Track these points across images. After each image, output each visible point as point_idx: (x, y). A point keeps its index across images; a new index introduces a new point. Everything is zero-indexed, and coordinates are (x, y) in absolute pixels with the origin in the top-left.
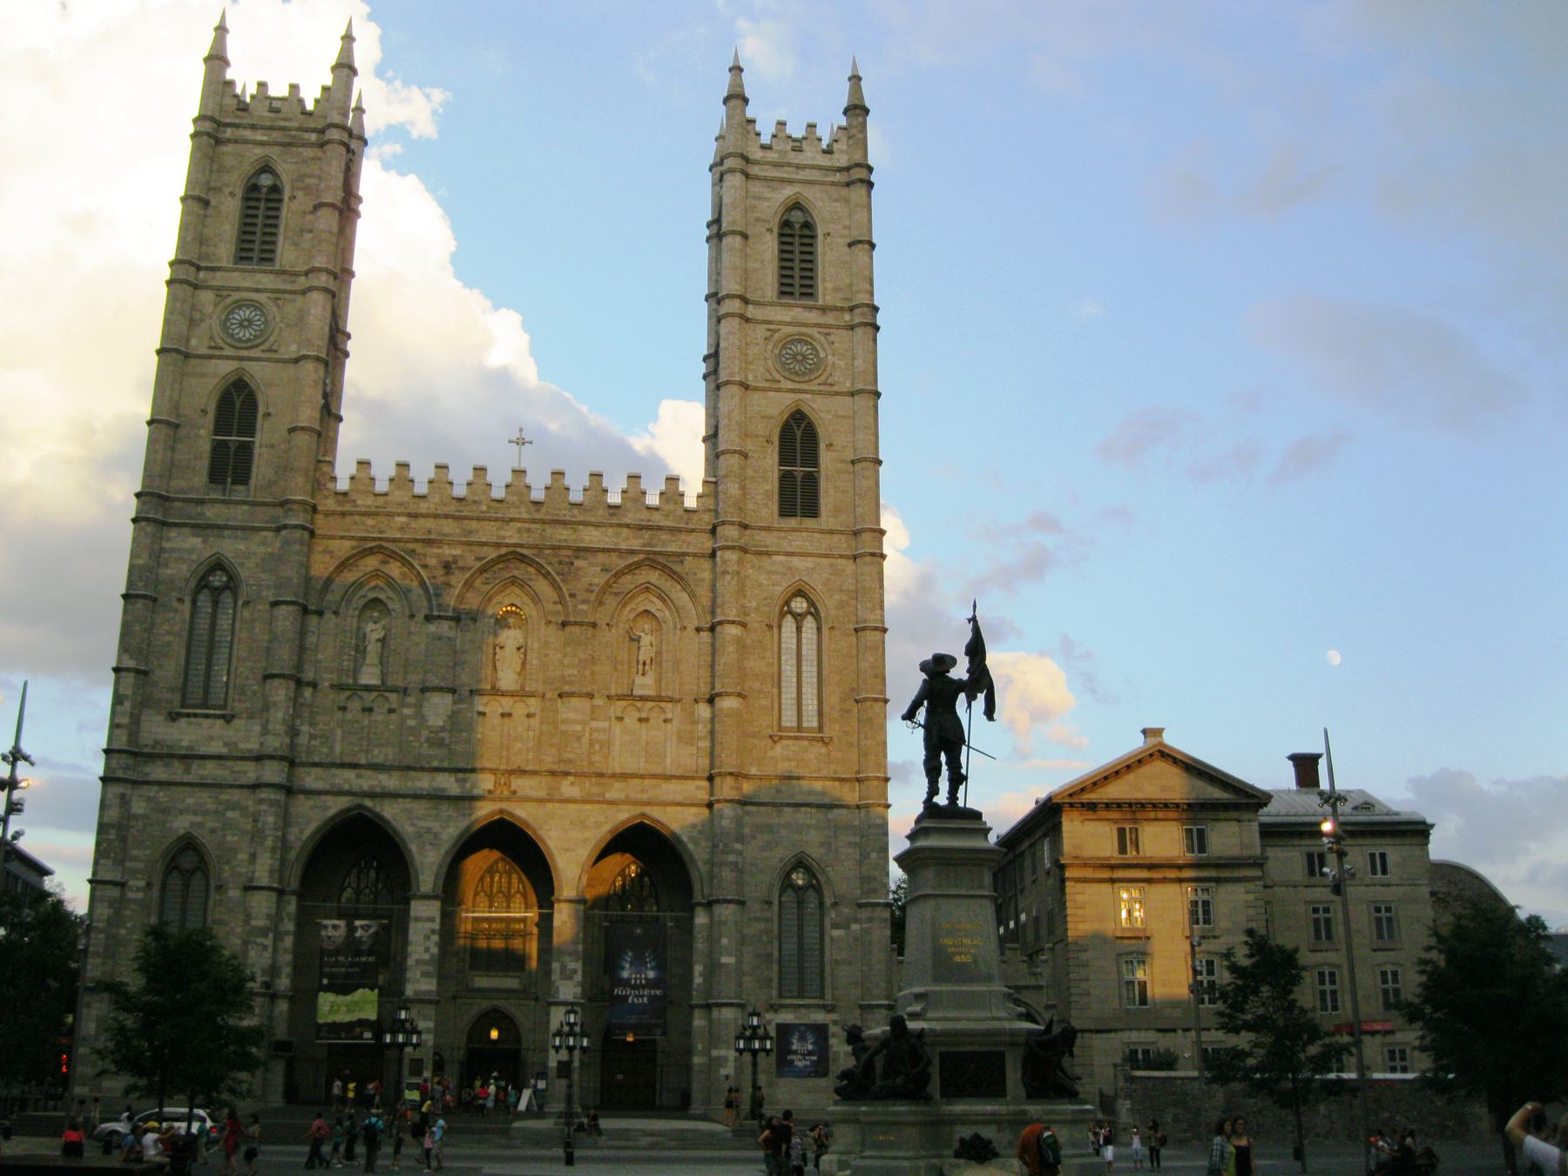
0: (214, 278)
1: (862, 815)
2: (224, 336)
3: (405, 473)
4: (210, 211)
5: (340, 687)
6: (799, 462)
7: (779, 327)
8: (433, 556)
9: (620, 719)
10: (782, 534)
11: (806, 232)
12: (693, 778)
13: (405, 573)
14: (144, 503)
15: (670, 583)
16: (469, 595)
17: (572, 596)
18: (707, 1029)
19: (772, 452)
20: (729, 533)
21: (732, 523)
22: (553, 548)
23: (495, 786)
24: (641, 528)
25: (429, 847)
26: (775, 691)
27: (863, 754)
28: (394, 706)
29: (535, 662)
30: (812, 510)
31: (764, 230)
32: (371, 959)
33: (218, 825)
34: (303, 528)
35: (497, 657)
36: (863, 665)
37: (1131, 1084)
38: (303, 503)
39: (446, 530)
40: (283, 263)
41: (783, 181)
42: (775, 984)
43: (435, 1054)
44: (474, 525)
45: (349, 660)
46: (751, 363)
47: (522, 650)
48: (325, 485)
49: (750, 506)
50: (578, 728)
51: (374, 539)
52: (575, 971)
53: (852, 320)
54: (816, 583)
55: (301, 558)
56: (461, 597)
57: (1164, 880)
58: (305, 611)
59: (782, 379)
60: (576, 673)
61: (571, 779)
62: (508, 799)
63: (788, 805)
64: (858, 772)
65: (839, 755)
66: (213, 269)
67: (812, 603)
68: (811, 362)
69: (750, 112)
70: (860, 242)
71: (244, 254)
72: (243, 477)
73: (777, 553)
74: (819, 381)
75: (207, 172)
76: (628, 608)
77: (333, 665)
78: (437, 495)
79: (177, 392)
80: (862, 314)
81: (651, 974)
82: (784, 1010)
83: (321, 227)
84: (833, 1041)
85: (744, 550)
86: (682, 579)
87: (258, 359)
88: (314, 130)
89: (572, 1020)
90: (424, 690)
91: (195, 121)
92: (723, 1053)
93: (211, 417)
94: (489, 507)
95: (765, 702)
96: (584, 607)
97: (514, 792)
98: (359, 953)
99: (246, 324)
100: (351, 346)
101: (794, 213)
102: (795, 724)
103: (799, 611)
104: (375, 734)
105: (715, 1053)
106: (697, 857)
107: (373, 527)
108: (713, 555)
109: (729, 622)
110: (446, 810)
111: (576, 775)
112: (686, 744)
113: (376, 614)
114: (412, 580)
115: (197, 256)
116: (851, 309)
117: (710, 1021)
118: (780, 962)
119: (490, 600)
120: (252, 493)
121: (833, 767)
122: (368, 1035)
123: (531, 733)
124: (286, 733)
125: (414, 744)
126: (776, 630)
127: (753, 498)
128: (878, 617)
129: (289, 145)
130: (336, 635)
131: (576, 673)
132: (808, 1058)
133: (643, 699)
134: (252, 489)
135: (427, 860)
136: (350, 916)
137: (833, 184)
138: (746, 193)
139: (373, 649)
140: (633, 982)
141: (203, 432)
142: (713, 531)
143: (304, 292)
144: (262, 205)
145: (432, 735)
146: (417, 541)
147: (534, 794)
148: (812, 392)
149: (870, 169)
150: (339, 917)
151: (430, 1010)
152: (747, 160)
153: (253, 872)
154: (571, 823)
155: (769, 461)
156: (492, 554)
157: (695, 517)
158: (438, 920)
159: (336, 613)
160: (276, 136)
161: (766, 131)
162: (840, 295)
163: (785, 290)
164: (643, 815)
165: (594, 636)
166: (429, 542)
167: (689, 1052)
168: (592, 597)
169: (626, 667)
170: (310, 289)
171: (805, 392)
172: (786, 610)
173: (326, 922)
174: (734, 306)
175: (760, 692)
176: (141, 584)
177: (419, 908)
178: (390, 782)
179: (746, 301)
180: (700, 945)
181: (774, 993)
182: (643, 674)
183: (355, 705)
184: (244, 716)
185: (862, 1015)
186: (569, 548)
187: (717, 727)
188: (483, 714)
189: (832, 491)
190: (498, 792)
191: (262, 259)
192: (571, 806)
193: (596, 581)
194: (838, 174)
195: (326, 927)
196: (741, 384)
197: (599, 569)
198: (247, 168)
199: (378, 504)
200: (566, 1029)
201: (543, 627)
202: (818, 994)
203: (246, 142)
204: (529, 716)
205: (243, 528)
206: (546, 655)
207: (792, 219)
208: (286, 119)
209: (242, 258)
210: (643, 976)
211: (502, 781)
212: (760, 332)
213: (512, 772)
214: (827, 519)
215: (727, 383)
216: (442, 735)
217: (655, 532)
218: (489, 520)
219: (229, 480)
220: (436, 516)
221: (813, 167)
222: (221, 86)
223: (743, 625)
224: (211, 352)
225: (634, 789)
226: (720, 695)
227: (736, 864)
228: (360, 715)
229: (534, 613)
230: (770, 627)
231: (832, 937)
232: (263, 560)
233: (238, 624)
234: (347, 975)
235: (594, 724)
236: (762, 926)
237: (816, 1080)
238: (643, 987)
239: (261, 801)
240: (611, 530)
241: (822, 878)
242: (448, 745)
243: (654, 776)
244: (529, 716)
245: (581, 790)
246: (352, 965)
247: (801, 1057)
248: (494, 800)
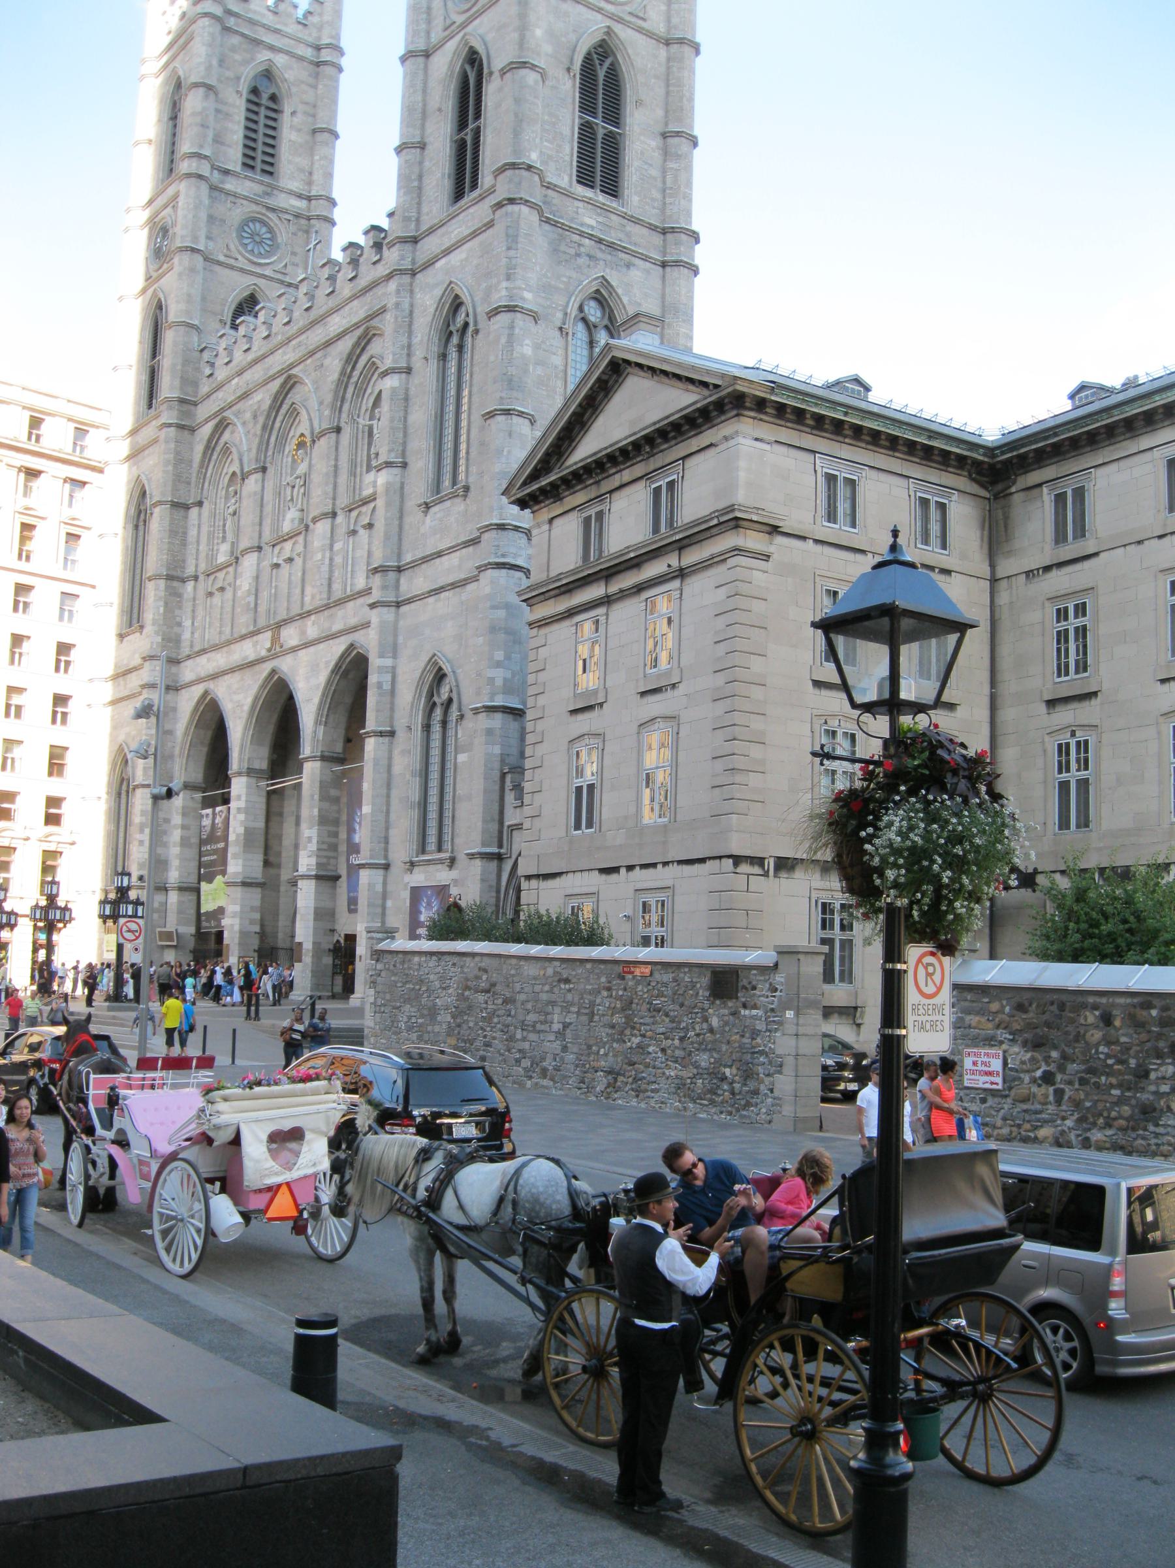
37: (377, 960)
39: (257, 376)
52: (310, 839)
55: (167, 456)
56: (263, 446)
57: (623, 595)
58: (180, 506)
61: (313, 617)
62: (275, 656)
87: (164, 274)
94: (283, 334)
124: (157, 633)
126: (433, 365)
128: (504, 293)
158: (244, 798)
166: (245, 396)
178: (219, 660)
204: (299, 555)
216: (248, 599)
230: (426, 359)
240: (347, 308)
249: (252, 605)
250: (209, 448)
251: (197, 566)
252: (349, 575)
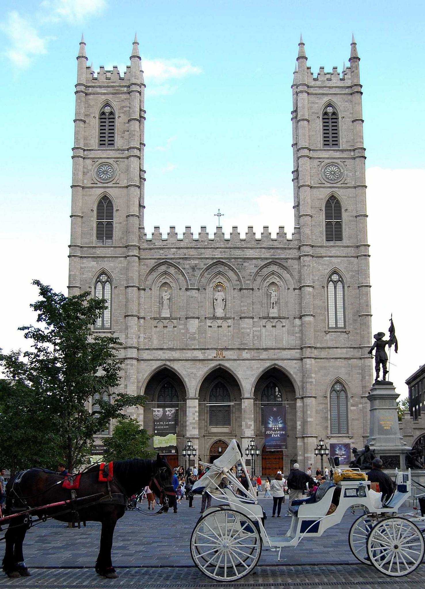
0: (91, 154)
1: (362, 362)
2: (97, 178)
3: (174, 231)
4: (86, 125)
5: (155, 319)
6: (333, 217)
7: (324, 160)
8: (187, 264)
9: (265, 326)
10: (328, 248)
11: (334, 117)
12: (294, 349)
13: (176, 271)
14: (72, 249)
15: (282, 270)
16: (202, 279)
17: (243, 277)
18: (303, 446)
19: (322, 214)
20: (306, 250)
21: (307, 245)
22: (235, 258)
24: (270, 248)
26: (326, 313)
27: (362, 337)
28: (175, 325)
29: (230, 305)
30: (339, 238)
31: (316, 117)
32: (173, 423)
34: (137, 256)
35: (215, 304)
36: (361, 301)
38: (135, 246)
40: (118, 146)
41: (323, 94)
42: (329, 429)
43: (199, 458)
44: (203, 251)
46: (313, 177)
47: (224, 300)
48: (142, 237)
49: (314, 237)
50: (248, 331)
51: (163, 259)
52: (251, 425)
53: (354, 155)
54: (342, 268)
58: (139, 289)
59: (326, 183)
61: (247, 351)
63: (333, 358)
64: (360, 345)
65: (353, 338)
66: (90, 150)
67: (340, 277)
68: (337, 174)
69: (308, 64)
70: (357, 120)
71: (102, 144)
72: (110, 236)
73: (326, 257)
74: (341, 182)
75: (84, 108)
76: (266, 282)
77: (151, 310)
78: (187, 239)
79: (81, 203)
80: (359, 152)
81: (280, 426)
82: (332, 438)
83: (132, 129)
85: (313, 257)
86: (287, 269)
87: (112, 187)
88: (125, 86)
89: (252, 444)
90: (186, 318)
91: (76, 86)
92: (309, 455)
93: (95, 212)
95: (321, 318)
96: (248, 282)
97: (225, 357)
99: (105, 172)
100: (146, 176)
101: (328, 108)
102: (334, 326)
103: (335, 280)
105: (306, 455)
106: (297, 380)
107: (163, 254)
108: (300, 258)
109: (307, 286)
110: (198, 364)
111: (248, 349)
113: (166, 289)
114: (179, 274)
115: (83, 145)
116: (354, 150)
117: (304, 443)
118: (331, 419)
119: (211, 281)
120: (114, 243)
121: (350, 343)
122: (173, 451)
123: (230, 333)
125: (184, 340)
126: (326, 288)
129: (115, 94)
130: (151, 298)
133: (273, 318)
134: (114, 241)
135: (192, 384)
136: (164, 407)
137: (345, 94)
138: (308, 101)
139: (166, 302)
140: (273, 429)
141: (92, 219)
142: (299, 248)
143: (127, 158)
144: (107, 121)
146: (180, 258)
147: (233, 358)
148: (339, 188)
149: (361, 86)
150: (159, 407)
151: (196, 441)
152: (308, 87)
153: (127, 392)
155: (322, 218)
156: (211, 262)
157: (292, 243)
158: (198, 407)
159: (150, 289)
160: (110, 90)
161: (315, 71)
162: (349, 144)
163: (326, 144)
164: (275, 364)
165: (253, 294)
166: (186, 259)
167: (296, 455)
168: (251, 279)
169: (266, 306)
170: (130, 156)
171: (336, 187)
172: (330, 280)
173: (154, 409)
174: (306, 152)
175: (321, 313)
176: (74, 282)
177: (189, 403)
178: (176, 355)
179: (310, 150)
180: (299, 414)
181: (329, 432)
182: (273, 308)
183: (160, 325)
184: (118, 332)
185: (364, 440)
186: (241, 258)
187: (303, 328)
188: (211, 327)
189: (347, 229)
190: (218, 357)
191: (109, 144)
192: (247, 361)
193: (253, 271)
194: (347, 89)
195: (155, 411)
196: (308, 186)
197: (253, 266)
198: (100, 106)
199: (164, 244)
200: (250, 448)
201: (232, 291)
202: (346, 432)
203: (98, 94)
204: (228, 327)
205: (112, 257)
206: (234, 302)
207: (328, 111)
208: (112, 82)
209: (101, 144)
210: (277, 426)
211: (220, 353)
212: (316, 162)
213: (222, 349)
214: (346, 241)
215: (303, 186)
216: (194, 336)
217: (275, 250)
218: (208, 248)
220: (187, 248)
221: (336, 87)
222: (85, 69)
223: (313, 287)
224: (92, 185)
225: (271, 354)
226: (304, 315)
227: (312, 382)
228: (163, 329)
229: (228, 285)
230: (323, 287)
231: (351, 410)
232: (121, 270)
233: (113, 296)
235: (254, 329)
236: (323, 406)
238: (278, 431)
239: (127, 364)
241: (346, 387)
242: (197, 339)
243: (279, 349)
244: (228, 327)
246: (166, 425)
247: (340, 456)
248: (216, 360)
249: (197, 338)
250: (153, 270)
251: (144, 313)
252: (264, 340)
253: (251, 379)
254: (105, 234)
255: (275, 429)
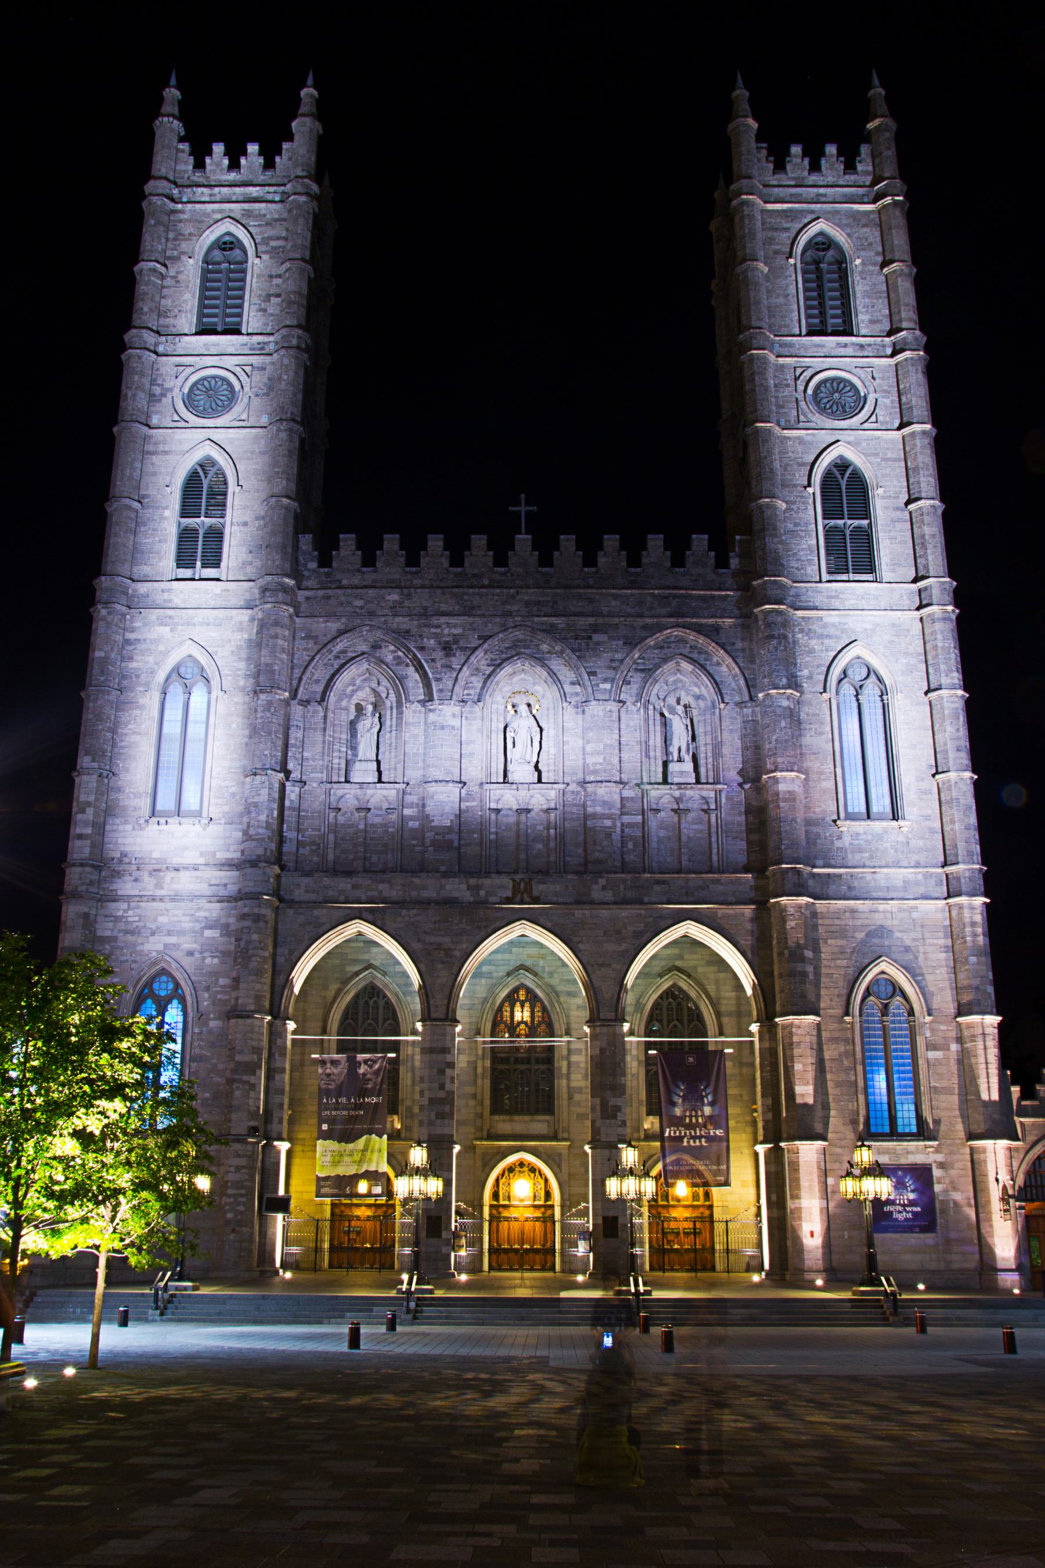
13: (399, 657)
23: (514, 893)
25: (439, 966)
33: (195, 946)
39: (444, 607)
45: (340, 758)
46: (783, 407)
50: (608, 823)
60: (601, 761)
65: (921, 843)
72: (213, 559)
78: (431, 571)
84: (937, 1188)
98: (364, 1093)
104: (372, 839)
107: (362, 608)
112: (737, 838)
114: (407, 665)
127: (795, 554)
130: (325, 729)
131: (601, 761)
132: (908, 1209)
140: (687, 1120)
145: (437, 837)
153: (237, 999)
154: (605, 933)
176: (102, 679)
184: (223, 821)
192: (604, 913)
197: (621, 643)
211: (522, 886)
216: (448, 837)
219: (199, 564)
234: (352, 1119)
236: (842, 1049)
237: (922, 1235)
245: (614, 895)
246: (358, 1107)
247: (900, 1208)
249: (456, 844)
253: (617, 967)
254: (199, 554)
255: (694, 1120)
